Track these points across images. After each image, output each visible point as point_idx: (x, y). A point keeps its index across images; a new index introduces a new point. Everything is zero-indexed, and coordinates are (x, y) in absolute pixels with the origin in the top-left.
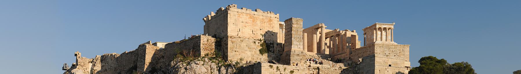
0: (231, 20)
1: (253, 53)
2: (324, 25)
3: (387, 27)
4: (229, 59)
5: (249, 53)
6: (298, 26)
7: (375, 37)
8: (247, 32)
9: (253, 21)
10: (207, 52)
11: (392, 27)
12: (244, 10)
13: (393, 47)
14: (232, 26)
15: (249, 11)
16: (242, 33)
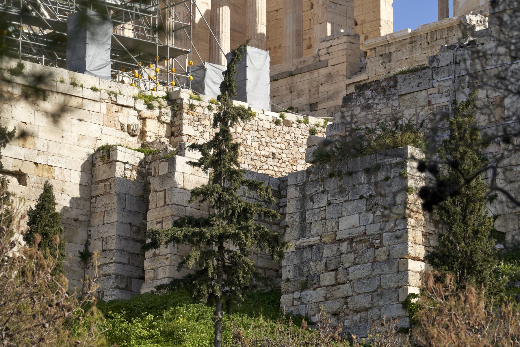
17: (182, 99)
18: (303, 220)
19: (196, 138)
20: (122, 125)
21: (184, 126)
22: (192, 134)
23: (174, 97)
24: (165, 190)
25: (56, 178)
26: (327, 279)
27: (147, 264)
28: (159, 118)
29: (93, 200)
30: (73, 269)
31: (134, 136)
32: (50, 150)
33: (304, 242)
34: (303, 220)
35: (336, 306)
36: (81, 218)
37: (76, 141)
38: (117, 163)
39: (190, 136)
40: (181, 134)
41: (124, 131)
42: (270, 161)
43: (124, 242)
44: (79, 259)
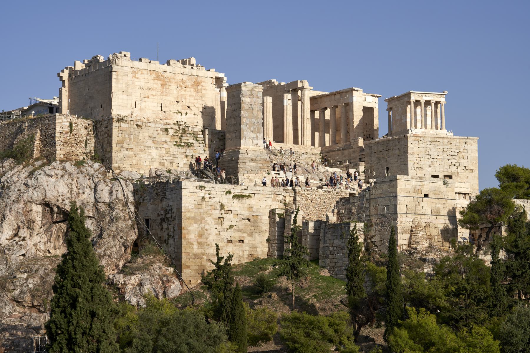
0: (118, 85)
1: (163, 152)
2: (306, 84)
3: (433, 98)
4: (114, 165)
5: (154, 153)
6: (254, 100)
7: (409, 120)
8: (149, 109)
9: (163, 85)
10: (68, 149)
11: (443, 100)
12: (144, 64)
13: (445, 141)
14: (121, 96)
15: (155, 65)
16: (141, 109)
18: (325, 239)
26: (331, 257)
33: (325, 245)
34: (325, 239)
35: (333, 265)
42: (324, 204)
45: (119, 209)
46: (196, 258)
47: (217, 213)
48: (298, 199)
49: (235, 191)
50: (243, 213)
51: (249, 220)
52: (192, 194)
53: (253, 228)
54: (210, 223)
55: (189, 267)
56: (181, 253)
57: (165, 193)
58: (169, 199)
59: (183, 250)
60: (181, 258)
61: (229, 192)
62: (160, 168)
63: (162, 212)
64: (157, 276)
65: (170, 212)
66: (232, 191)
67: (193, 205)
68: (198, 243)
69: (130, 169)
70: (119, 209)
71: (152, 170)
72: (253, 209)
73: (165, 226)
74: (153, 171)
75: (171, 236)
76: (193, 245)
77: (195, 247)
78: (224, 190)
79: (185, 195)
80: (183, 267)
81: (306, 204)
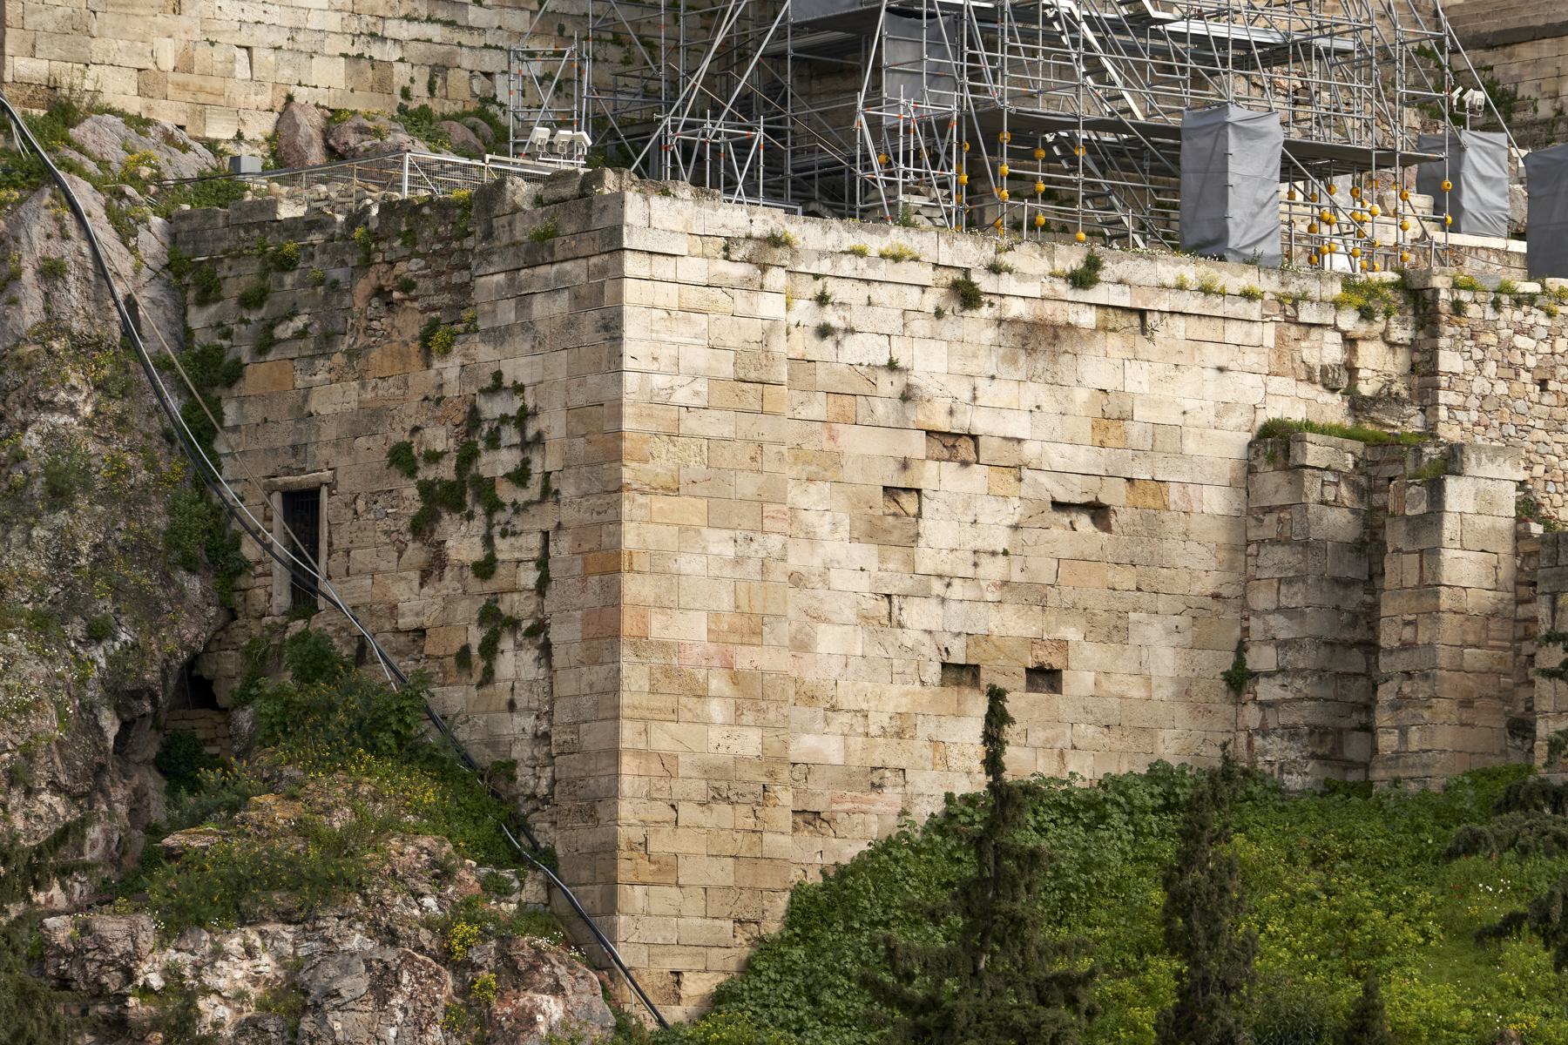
17: (1436, 291)
19: (1468, 378)
20: (1310, 370)
21: (1441, 353)
22: (1458, 369)
23: (1417, 283)
24: (1422, 551)
25: (1172, 507)
27: (1383, 718)
28: (1384, 336)
29: (1252, 549)
30: (1212, 707)
31: (1334, 391)
32: (1158, 445)
36: (1225, 592)
37: (1212, 418)
38: (1307, 471)
39: (1455, 374)
40: (1436, 373)
41: (1314, 383)
43: (1324, 651)
44: (1223, 685)
45: (71, 409)
46: (718, 796)
47: (870, 450)
48: (1449, 361)
49: (1007, 284)
50: (1057, 456)
51: (1098, 512)
52: (694, 297)
53: (1125, 579)
54: (823, 529)
55: (666, 871)
56: (615, 754)
57: (465, 289)
58: (498, 336)
59: (628, 733)
60: (613, 794)
61: (966, 295)
62: (360, 103)
63: (439, 438)
64: (425, 935)
65: (509, 435)
66: (984, 282)
67: (702, 386)
68: (736, 678)
69: (134, 106)
70: (71, 409)
71: (302, 119)
72: (1134, 430)
73: (462, 541)
74: (309, 124)
75: (514, 624)
76: (702, 695)
77: (717, 710)
78: (925, 275)
79: (643, 295)
80: (624, 869)
81: (1501, 403)
